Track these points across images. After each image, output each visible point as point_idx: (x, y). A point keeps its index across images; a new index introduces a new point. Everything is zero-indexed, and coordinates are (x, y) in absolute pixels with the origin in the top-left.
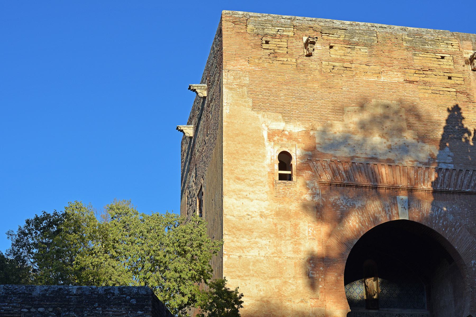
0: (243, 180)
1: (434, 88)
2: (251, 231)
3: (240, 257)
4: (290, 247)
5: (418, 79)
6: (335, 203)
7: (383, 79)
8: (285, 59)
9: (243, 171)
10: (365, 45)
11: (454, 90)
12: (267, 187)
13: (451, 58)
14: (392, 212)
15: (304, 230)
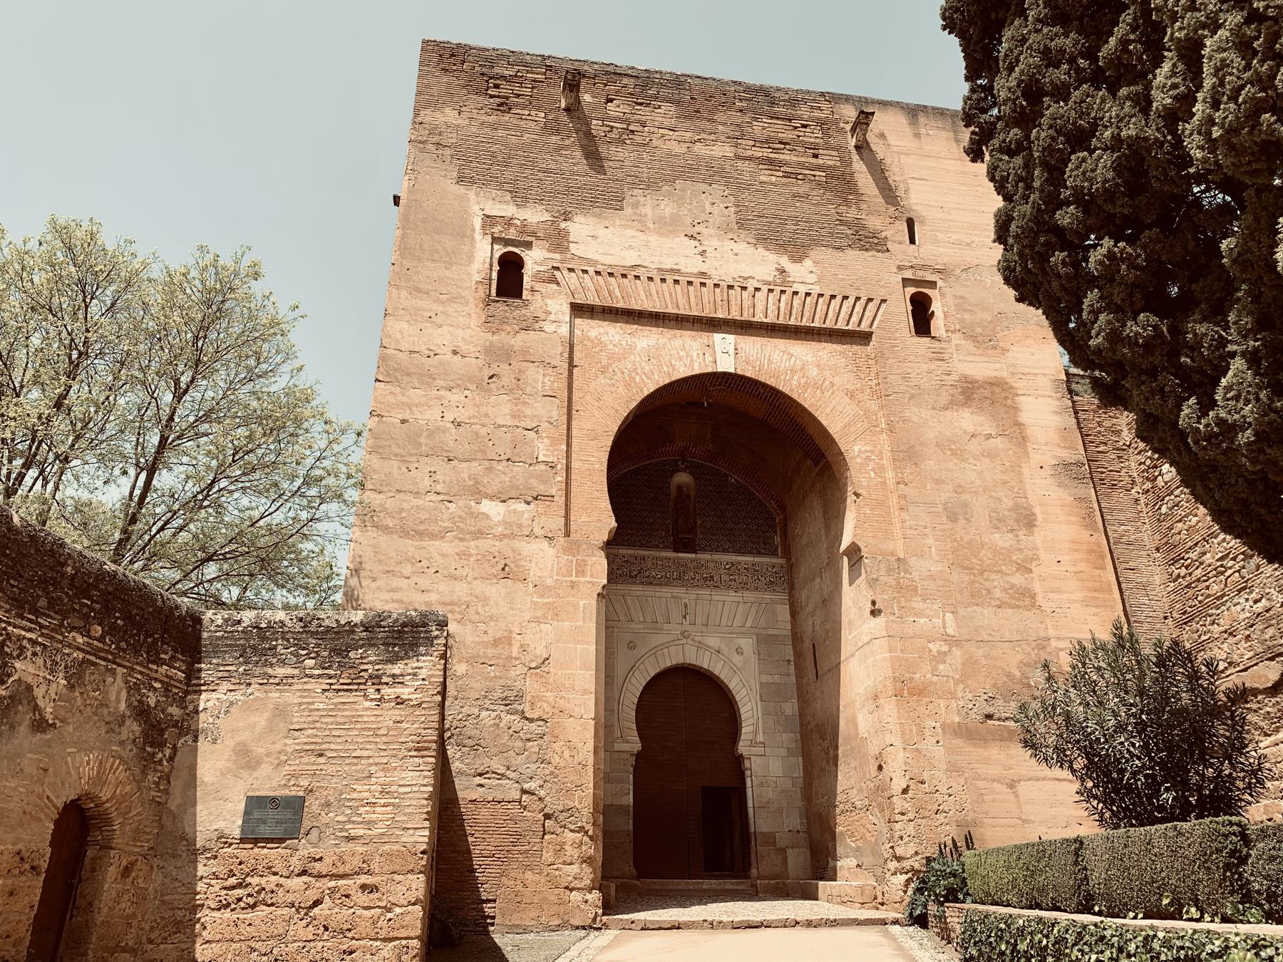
1: (789, 170)
3: (403, 422)
4: (506, 409)
5: (761, 154)
7: (697, 148)
8: (527, 112)
9: (428, 277)
11: (824, 174)
12: (472, 305)
15: (536, 381)
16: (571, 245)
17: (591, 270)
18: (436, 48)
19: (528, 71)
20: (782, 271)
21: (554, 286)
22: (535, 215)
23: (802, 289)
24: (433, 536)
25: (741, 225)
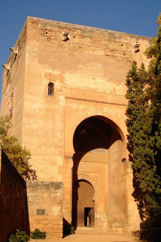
0: (33, 94)
2: (35, 116)
3: (30, 127)
5: (111, 54)
6: (71, 107)
7: (96, 53)
8: (54, 41)
10: (89, 37)
11: (126, 60)
13: (126, 46)
14: (95, 112)
16: (65, 81)
17: (70, 88)
18: (31, 21)
19: (54, 28)
20: (114, 89)
21: (61, 92)
22: (57, 73)
23: (118, 93)
24: (37, 155)
25: (105, 75)
